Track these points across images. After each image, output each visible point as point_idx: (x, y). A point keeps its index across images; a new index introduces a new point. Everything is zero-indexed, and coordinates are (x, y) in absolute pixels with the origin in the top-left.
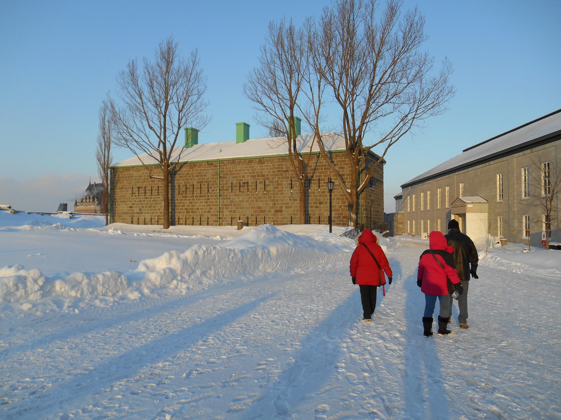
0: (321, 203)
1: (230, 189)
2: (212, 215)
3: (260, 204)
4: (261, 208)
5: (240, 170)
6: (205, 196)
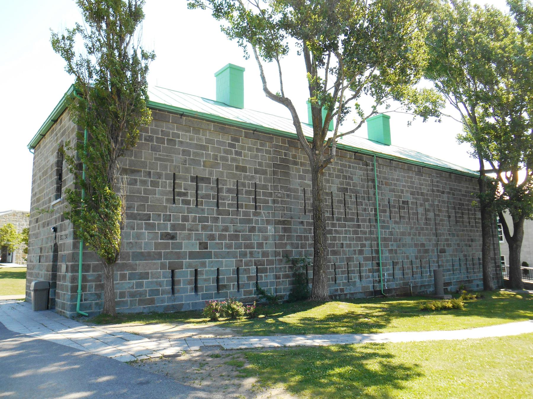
0: (472, 241)
1: (388, 210)
2: (366, 259)
3: (422, 239)
4: (423, 245)
5: (398, 180)
6: (352, 220)
